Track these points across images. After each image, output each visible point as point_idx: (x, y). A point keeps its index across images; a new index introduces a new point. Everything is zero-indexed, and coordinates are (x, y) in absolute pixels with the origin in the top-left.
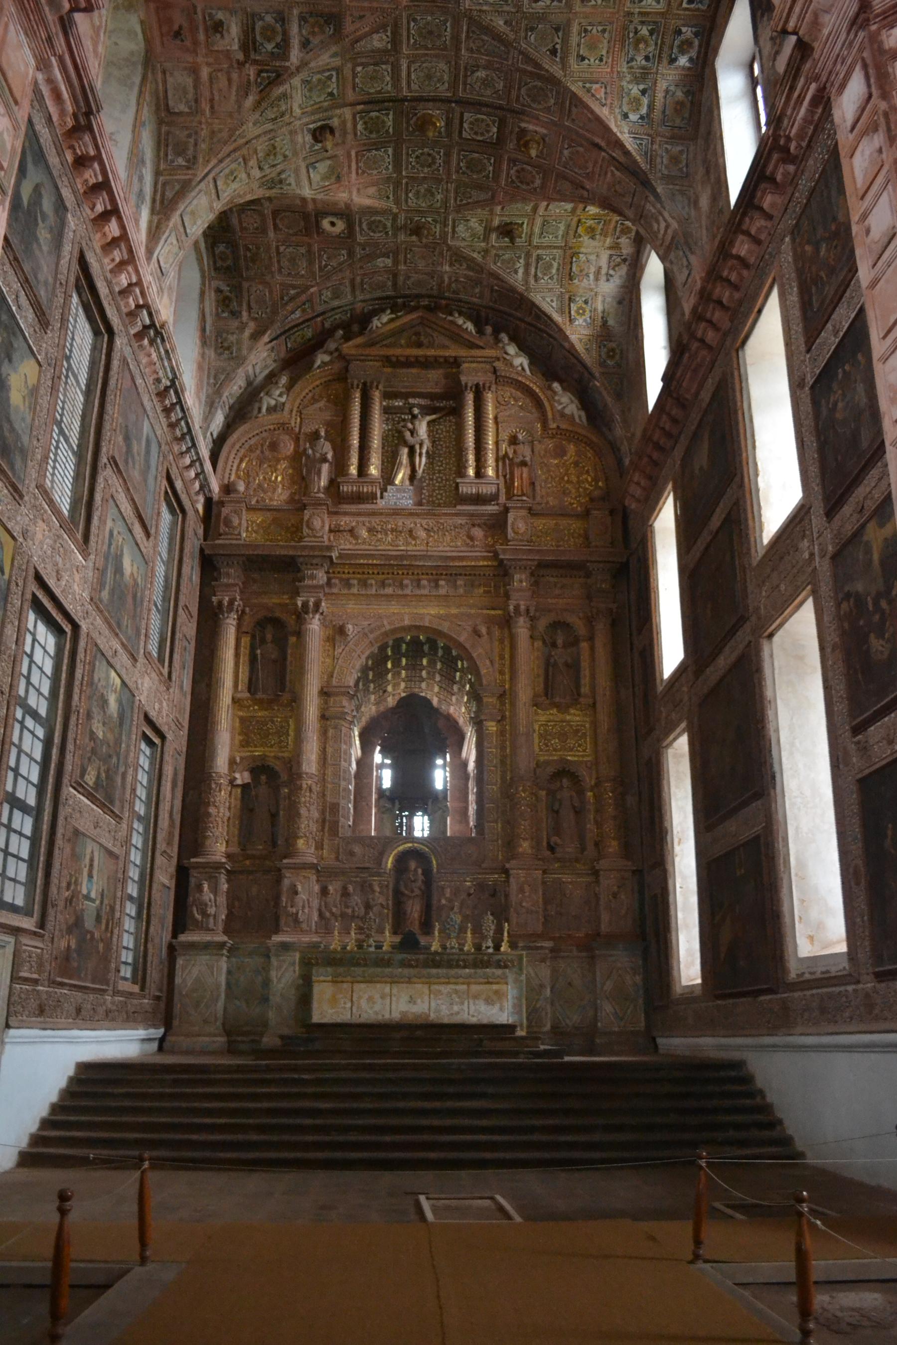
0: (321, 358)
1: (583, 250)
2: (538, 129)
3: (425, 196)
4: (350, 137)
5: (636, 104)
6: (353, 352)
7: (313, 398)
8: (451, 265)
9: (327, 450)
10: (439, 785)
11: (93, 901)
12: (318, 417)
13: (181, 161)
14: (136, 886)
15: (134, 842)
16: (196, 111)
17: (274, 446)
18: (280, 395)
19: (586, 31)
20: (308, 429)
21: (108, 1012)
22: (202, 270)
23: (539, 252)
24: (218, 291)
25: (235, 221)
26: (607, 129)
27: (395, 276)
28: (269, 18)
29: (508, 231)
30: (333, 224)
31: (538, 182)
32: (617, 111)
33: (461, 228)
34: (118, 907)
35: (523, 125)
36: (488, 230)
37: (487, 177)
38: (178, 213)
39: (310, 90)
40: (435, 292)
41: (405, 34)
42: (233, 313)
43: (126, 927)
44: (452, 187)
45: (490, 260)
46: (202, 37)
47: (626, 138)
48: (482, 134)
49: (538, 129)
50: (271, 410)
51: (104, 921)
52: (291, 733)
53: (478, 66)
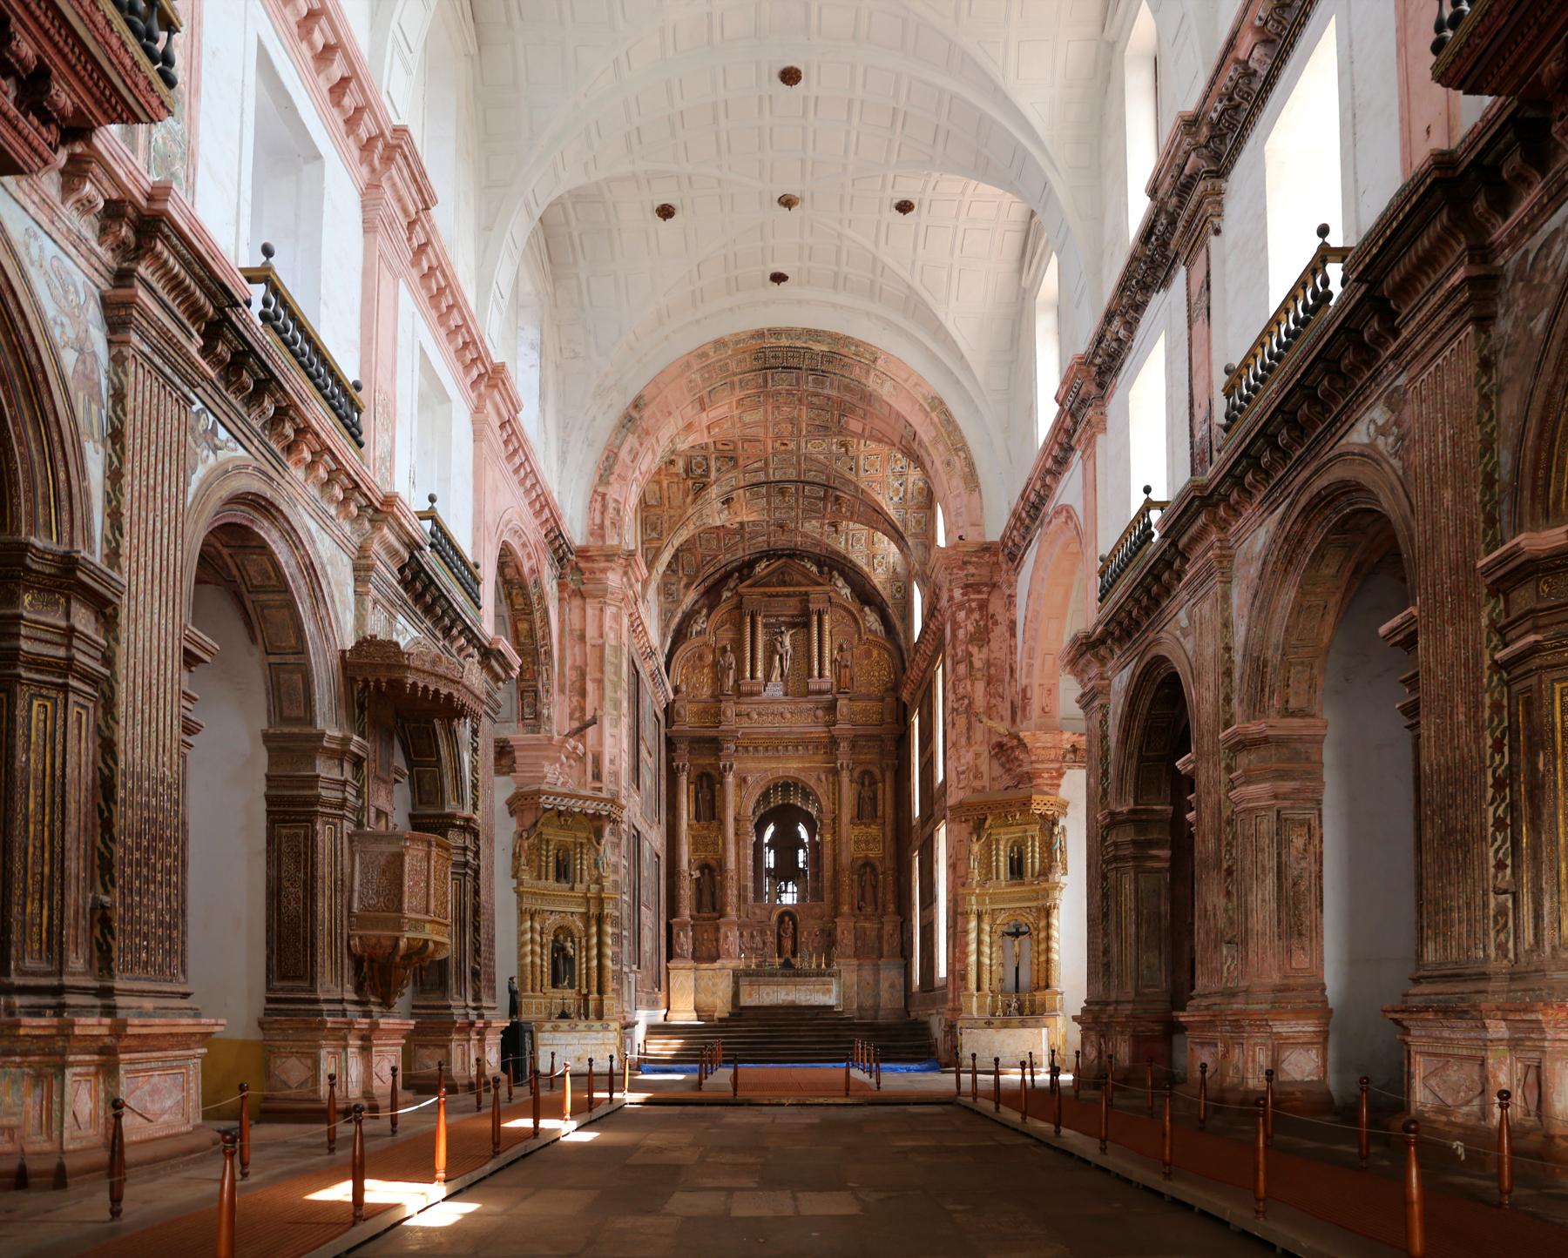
9: (731, 658)
12: (726, 637)
50: (699, 633)
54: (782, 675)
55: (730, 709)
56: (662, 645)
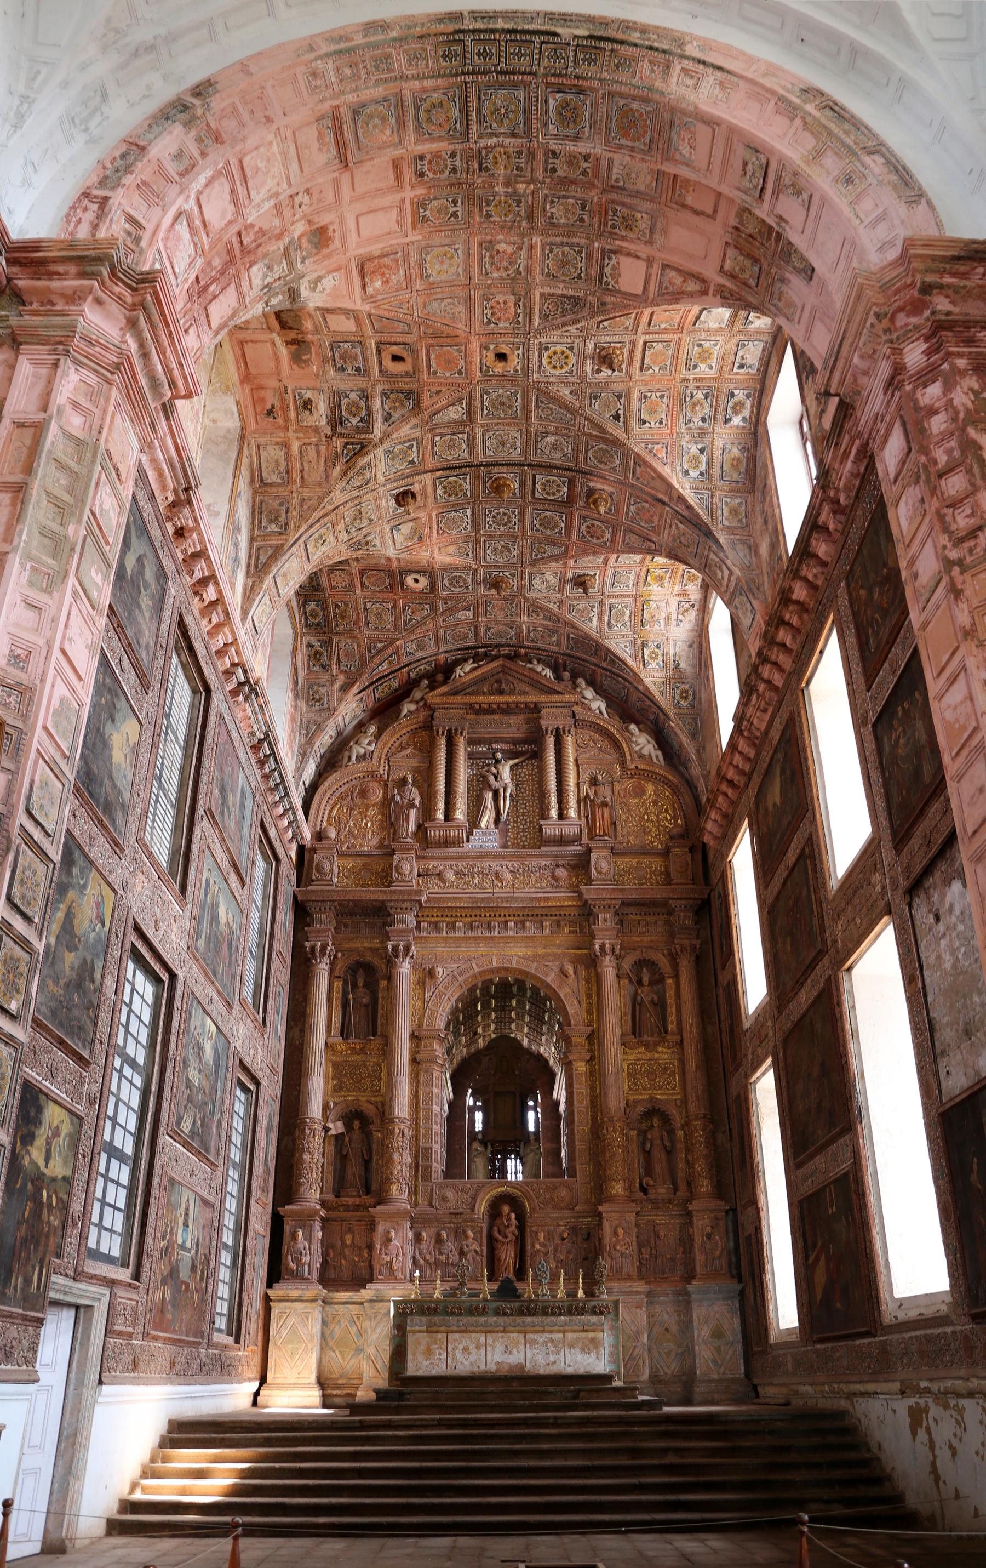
0: (407, 707)
1: (652, 597)
2: (606, 487)
3: (502, 552)
4: (430, 501)
5: (695, 461)
6: (437, 700)
7: (400, 745)
8: (528, 615)
10: (531, 1128)
11: (189, 1251)
13: (274, 527)
14: (231, 1234)
15: (229, 1189)
16: (287, 480)
17: (363, 793)
18: (369, 744)
19: (645, 397)
20: (395, 776)
21: (202, 1366)
22: (294, 628)
23: (612, 601)
24: (310, 646)
25: (324, 580)
26: (670, 486)
27: (476, 627)
28: (353, 396)
29: (581, 582)
30: (416, 581)
31: (608, 536)
32: (678, 468)
33: (536, 581)
34: (213, 1257)
35: (591, 484)
36: (563, 582)
37: (560, 533)
38: (272, 575)
39: (393, 459)
40: (514, 641)
41: (479, 405)
42: (323, 666)
43: (221, 1277)
44: (526, 544)
45: (566, 609)
46: (292, 414)
47: (688, 494)
48: (554, 494)
49: (606, 487)
51: (199, 1272)
52: (384, 1075)
53: (547, 433)
54: (497, 821)
55: (408, 866)
56: (300, 768)
